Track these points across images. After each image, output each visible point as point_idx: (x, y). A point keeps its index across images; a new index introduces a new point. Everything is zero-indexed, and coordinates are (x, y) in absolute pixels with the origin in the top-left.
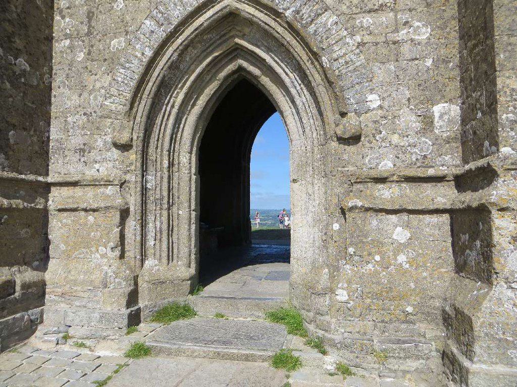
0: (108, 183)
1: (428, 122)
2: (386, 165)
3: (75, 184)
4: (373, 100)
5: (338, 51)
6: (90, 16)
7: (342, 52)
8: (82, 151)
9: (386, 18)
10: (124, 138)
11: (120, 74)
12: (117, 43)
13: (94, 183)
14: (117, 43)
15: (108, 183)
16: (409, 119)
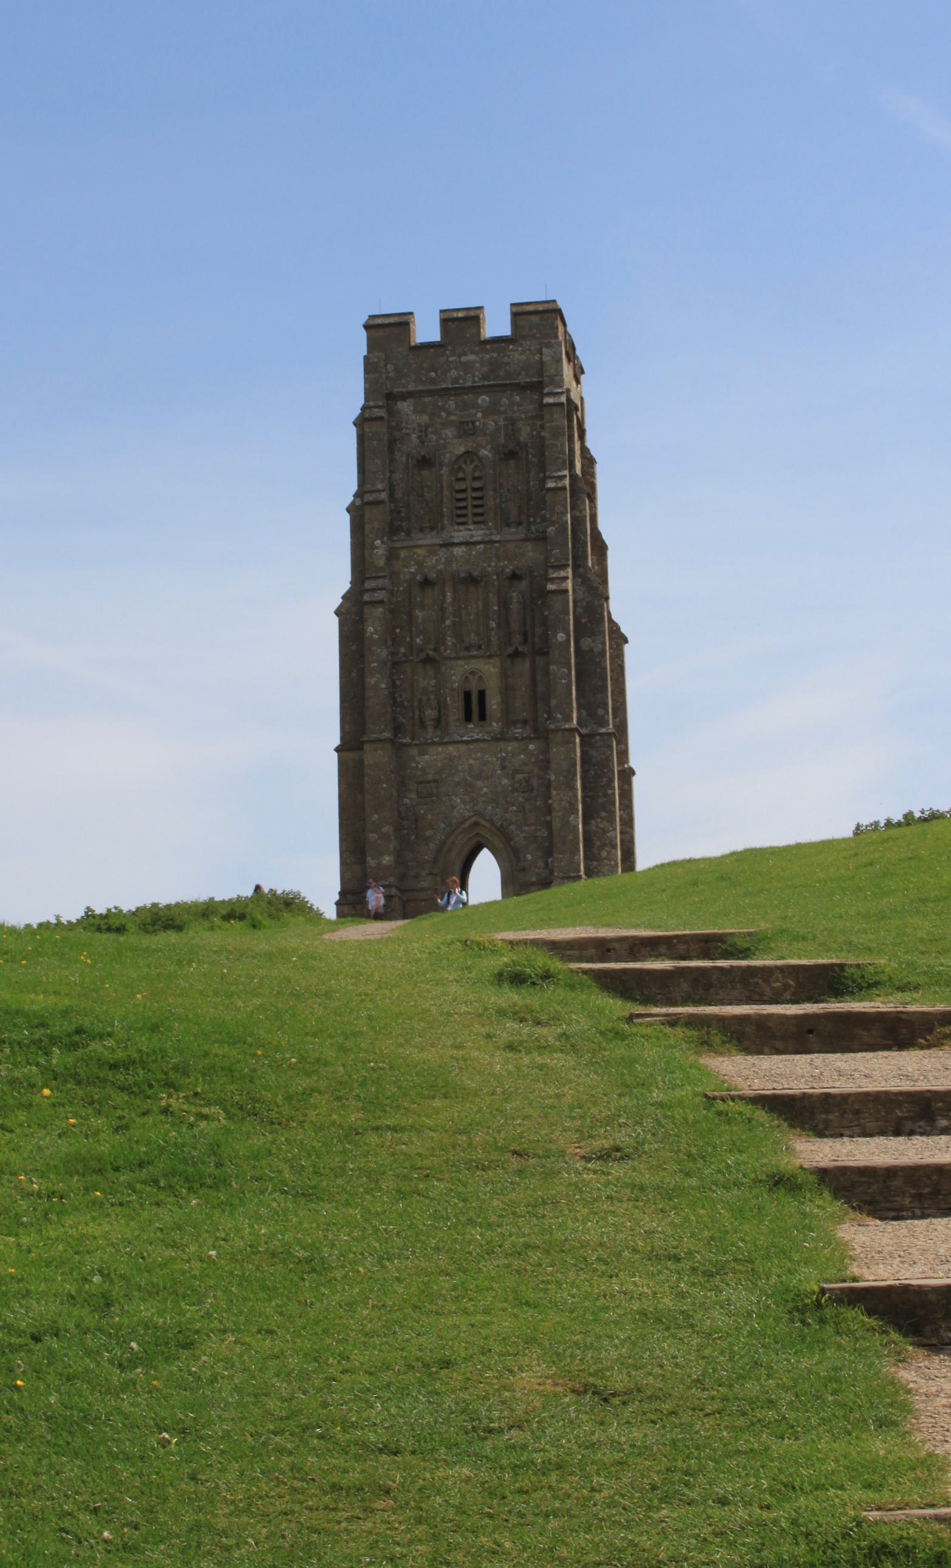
0: (428, 889)
1: (547, 864)
2: (534, 879)
3: (412, 890)
4: (529, 857)
5: (517, 839)
6: (416, 820)
7: (519, 839)
8: (416, 877)
9: (533, 828)
10: (435, 871)
11: (432, 846)
12: (429, 833)
13: (423, 890)
14: (429, 833)
15: (428, 889)
16: (541, 864)
